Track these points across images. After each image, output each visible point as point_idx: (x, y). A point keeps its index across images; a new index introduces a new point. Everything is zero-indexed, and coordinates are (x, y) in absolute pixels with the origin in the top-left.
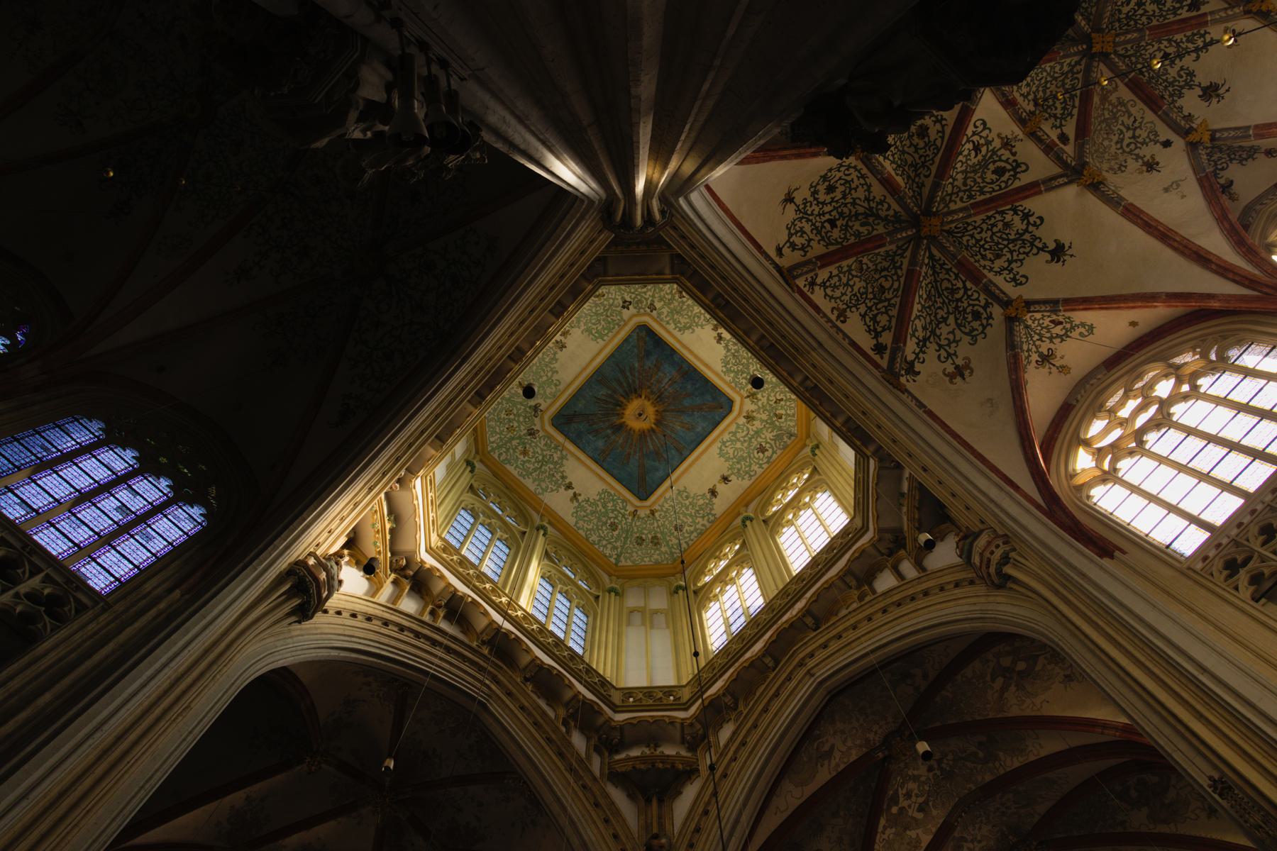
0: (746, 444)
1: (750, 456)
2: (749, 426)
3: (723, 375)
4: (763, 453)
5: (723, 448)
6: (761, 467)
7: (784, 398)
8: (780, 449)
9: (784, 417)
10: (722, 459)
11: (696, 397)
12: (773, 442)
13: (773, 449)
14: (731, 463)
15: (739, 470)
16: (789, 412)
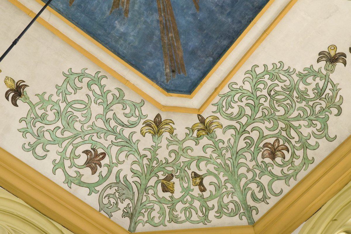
0: (100, 124)
1: (75, 137)
2: (141, 125)
3: (247, 66)
4: (88, 164)
5: (86, 80)
6: (57, 165)
7: (206, 194)
8: (100, 202)
9: (167, 195)
10: (60, 80)
11: (194, 15)
12: (112, 179)
13: (98, 184)
14: (55, 98)
15: (43, 117)
16: (179, 206)
